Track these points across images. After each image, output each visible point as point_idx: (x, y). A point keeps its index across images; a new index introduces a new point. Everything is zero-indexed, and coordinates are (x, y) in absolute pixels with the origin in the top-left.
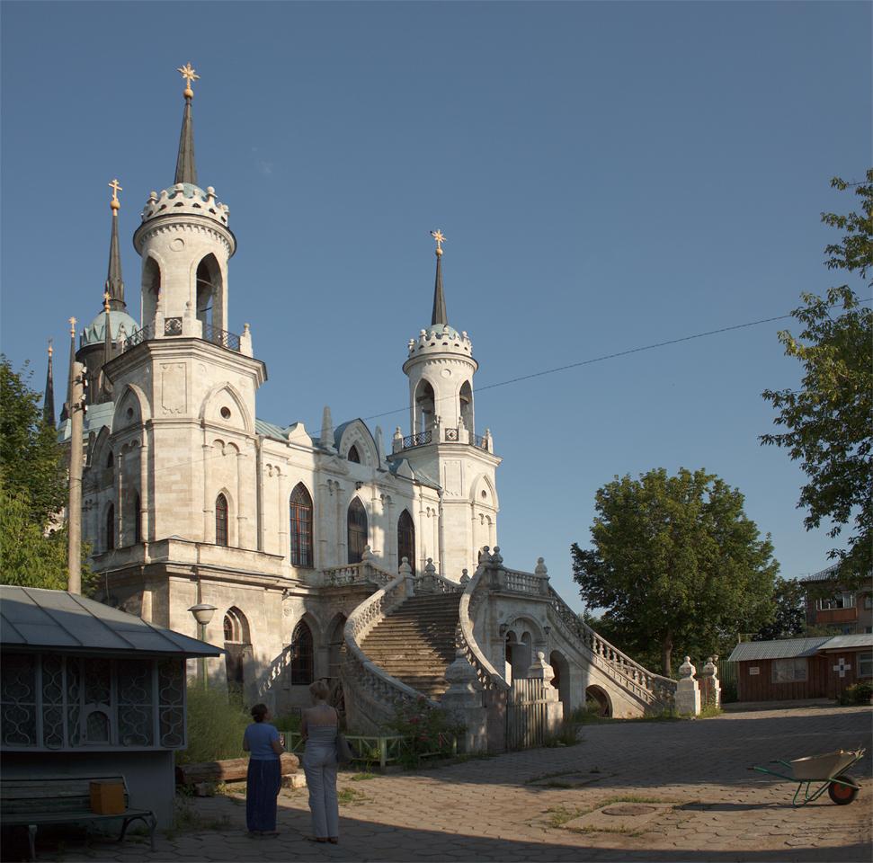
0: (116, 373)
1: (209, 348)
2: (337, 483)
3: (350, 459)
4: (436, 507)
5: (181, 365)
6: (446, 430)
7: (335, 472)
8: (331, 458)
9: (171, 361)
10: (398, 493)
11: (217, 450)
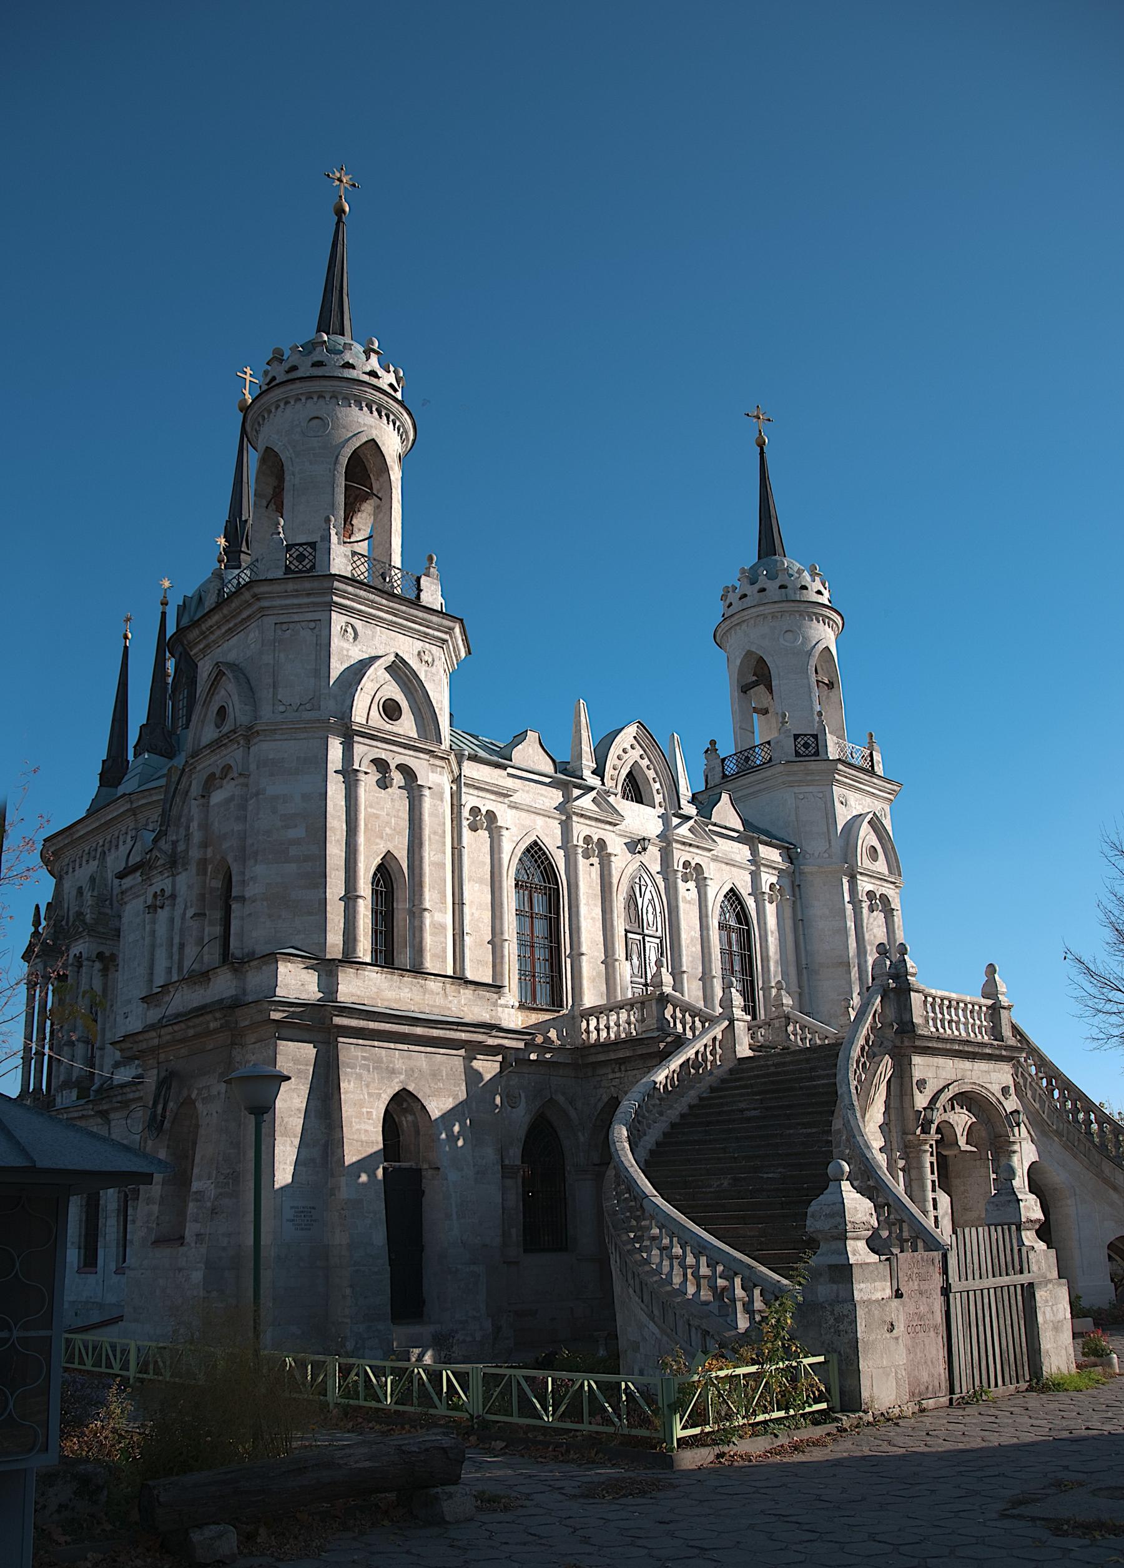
0: (201, 646)
1: (362, 593)
3: (625, 796)
5: (312, 625)
6: (796, 737)
9: (296, 618)
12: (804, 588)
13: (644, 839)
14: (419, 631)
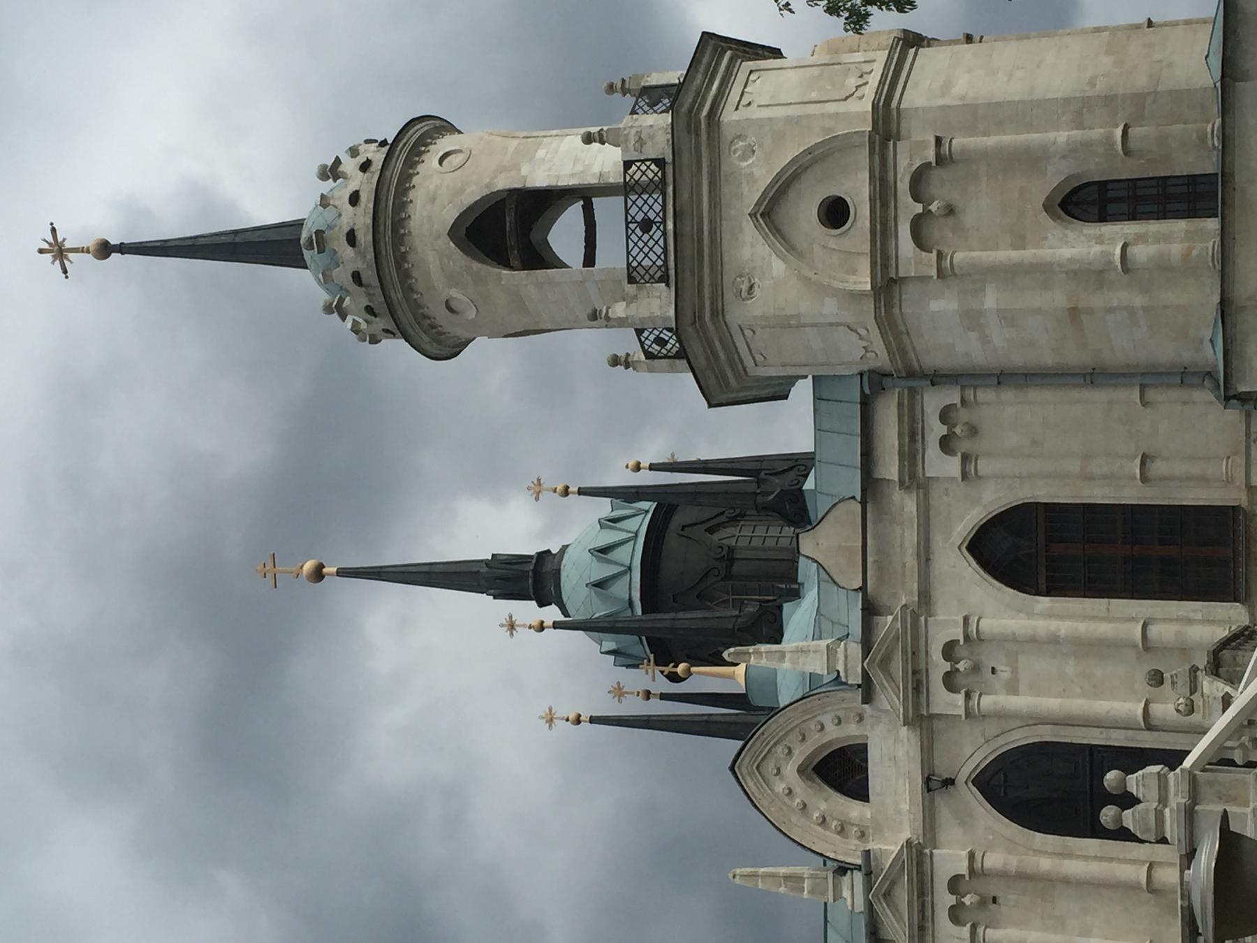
2: (955, 884)
4: (933, 401)
7: (922, 894)
8: (884, 911)
10: (925, 597)
12: (356, 277)
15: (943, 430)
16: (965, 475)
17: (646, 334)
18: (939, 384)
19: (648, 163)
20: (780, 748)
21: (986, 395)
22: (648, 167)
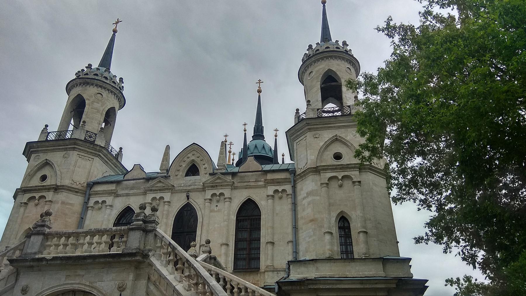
1: (39, 144)
2: (162, 198)
4: (288, 188)
11: (32, 204)
13: (189, 191)
14: (63, 148)
15: (280, 190)
16: (268, 196)
17: (304, 115)
18: (292, 188)
19: (350, 111)
20: (199, 155)
21: (290, 200)
22: (349, 111)
